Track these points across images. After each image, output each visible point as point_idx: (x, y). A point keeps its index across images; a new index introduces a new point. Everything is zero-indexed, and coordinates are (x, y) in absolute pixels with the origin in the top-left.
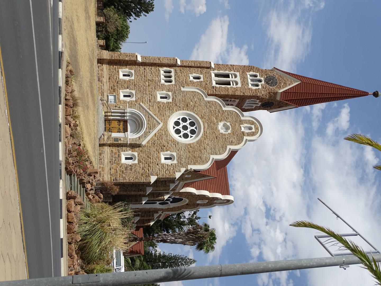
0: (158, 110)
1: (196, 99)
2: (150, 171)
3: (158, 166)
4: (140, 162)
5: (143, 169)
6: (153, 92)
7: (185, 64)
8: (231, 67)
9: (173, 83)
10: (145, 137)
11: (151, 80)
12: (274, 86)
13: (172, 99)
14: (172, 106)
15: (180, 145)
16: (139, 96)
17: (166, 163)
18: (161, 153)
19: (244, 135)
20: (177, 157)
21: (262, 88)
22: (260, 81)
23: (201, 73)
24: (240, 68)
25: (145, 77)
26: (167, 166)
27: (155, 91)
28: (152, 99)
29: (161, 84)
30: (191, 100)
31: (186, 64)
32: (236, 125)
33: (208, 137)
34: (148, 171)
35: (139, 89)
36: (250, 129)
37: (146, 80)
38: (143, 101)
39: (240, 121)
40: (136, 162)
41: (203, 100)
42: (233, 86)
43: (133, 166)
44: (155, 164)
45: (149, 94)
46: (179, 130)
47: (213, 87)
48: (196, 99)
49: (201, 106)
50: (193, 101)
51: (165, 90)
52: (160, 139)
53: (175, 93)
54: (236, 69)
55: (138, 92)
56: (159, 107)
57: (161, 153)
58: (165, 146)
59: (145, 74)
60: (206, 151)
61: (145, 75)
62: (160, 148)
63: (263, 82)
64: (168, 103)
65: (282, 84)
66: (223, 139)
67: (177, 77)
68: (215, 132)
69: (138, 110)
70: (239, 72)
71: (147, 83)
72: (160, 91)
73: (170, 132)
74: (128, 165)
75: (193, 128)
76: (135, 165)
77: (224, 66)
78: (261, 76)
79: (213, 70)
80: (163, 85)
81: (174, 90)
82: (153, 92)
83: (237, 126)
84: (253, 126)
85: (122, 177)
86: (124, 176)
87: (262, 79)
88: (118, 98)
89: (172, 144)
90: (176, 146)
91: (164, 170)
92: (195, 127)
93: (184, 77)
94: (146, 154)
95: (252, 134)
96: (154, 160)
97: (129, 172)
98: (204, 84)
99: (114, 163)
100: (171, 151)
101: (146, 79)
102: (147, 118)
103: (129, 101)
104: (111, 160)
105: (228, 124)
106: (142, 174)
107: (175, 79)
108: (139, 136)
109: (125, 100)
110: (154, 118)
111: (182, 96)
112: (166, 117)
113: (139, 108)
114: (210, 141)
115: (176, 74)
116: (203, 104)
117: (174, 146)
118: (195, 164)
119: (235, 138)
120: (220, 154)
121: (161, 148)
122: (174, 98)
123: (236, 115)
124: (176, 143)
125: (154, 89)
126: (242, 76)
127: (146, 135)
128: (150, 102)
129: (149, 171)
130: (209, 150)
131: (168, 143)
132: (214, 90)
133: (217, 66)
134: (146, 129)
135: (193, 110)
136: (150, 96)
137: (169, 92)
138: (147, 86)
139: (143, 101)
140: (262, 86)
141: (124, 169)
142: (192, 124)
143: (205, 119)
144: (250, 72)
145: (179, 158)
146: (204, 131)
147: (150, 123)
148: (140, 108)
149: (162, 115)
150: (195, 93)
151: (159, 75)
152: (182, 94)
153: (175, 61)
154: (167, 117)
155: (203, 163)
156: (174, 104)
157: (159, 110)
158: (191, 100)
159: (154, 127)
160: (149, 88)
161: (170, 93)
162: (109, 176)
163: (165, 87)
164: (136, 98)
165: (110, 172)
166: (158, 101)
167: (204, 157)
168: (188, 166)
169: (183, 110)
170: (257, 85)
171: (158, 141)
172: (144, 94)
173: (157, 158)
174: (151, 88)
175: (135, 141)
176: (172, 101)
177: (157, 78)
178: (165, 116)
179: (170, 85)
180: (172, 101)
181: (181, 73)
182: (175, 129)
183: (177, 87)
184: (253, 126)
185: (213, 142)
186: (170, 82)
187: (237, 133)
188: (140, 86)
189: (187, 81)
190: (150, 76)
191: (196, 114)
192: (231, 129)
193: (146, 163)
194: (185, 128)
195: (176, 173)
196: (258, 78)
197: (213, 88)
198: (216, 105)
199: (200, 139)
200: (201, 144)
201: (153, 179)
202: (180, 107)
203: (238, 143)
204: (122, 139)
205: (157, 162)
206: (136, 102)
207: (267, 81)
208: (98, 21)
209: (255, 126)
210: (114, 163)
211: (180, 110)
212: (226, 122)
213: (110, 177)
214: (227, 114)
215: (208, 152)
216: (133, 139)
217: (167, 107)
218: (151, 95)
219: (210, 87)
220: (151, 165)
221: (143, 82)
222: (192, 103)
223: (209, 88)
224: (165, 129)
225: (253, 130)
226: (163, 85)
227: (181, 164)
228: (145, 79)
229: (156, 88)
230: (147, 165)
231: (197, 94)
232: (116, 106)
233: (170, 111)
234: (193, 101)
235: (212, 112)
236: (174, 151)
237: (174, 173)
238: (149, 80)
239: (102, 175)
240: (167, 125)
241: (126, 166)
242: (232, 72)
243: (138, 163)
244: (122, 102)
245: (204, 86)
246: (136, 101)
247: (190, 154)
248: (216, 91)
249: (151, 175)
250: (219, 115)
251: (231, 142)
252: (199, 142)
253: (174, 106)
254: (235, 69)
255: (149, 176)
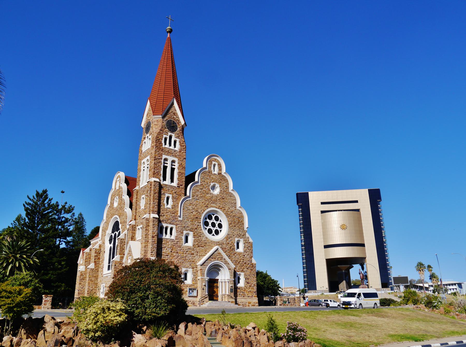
0: (201, 247)
1: (191, 208)
2: (249, 263)
3: (245, 256)
4: (243, 270)
5: (248, 269)
6: (184, 249)
7: (156, 210)
8: (157, 160)
9: (174, 226)
10: (228, 264)
11: (172, 250)
12: (177, 126)
13: (190, 231)
14: (197, 233)
15: (230, 233)
16: (188, 264)
17: (243, 248)
18: (236, 251)
19: (221, 174)
20: (239, 238)
21: (179, 139)
22: (171, 137)
23: (164, 194)
24: (159, 151)
25: (168, 256)
26: (245, 247)
27: (183, 248)
28: (190, 252)
29: (176, 240)
30: (191, 213)
31: (155, 208)
32: (213, 178)
33: (224, 207)
34: (249, 265)
35: (181, 263)
36: (214, 165)
37: (171, 254)
38: (192, 261)
39: (209, 172)
40: (242, 274)
41: (191, 201)
42: (176, 166)
43: (245, 277)
44: (244, 257)
45: (186, 254)
46: (215, 230)
47: (178, 187)
48: (191, 208)
49: (197, 205)
50: (192, 211)
51: (181, 237)
52: (225, 250)
53: (185, 227)
54: (159, 156)
55: (184, 265)
56: (199, 246)
57: (236, 251)
58: (231, 247)
59: (165, 255)
60: (234, 211)
61: (166, 255)
62: (232, 251)
63: (173, 135)
64: (194, 236)
65: (175, 117)
66: (224, 193)
67: (168, 221)
68: (219, 199)
69: (206, 268)
70: (162, 154)
71: (174, 254)
72: (182, 242)
73: (220, 240)
74: (245, 281)
75: (213, 217)
76: (245, 275)
77: (155, 167)
78: (166, 134)
79: (160, 180)
80: (177, 238)
81: (182, 228)
82: (184, 249)
83: (214, 177)
84: (213, 163)
85: (254, 287)
86: (253, 285)
87: (169, 134)
88: (190, 286)
89: (229, 240)
90: (231, 237)
91: (248, 251)
92: (212, 215)
93: (168, 214)
94: (237, 264)
95: (219, 166)
96: (241, 258)
97: (250, 281)
98: (176, 195)
99: (244, 293)
100: (234, 242)
101: (170, 255)
102: (212, 260)
103: (193, 275)
104: (242, 296)
105: (212, 184)
106: (251, 270)
107: (170, 223)
108: (228, 270)
109: (192, 279)
110: (213, 253)
111: (187, 221)
112: (207, 241)
113: (205, 267)
114: (226, 205)
115: (165, 222)
116: (195, 202)
117: (231, 238)
118: (243, 224)
119: (223, 182)
120: (236, 200)
121: (233, 250)
122: (190, 230)
123: (204, 174)
124: (228, 237)
125: (181, 247)
126: (167, 153)
127: (226, 263)
128: (193, 254)
129: (249, 264)
130: (233, 209)
131: (229, 243)
132: (181, 186)
133: (156, 175)
134: (222, 262)
135: (200, 214)
136: (187, 253)
137: (183, 233)
138: (177, 254)
139: (192, 261)
140: (177, 138)
141: (248, 285)
142: (210, 217)
143: (208, 204)
144: (162, 143)
145: (239, 236)
146: (219, 208)
147: (217, 257)
148: (204, 265)
149: (205, 244)
150: (185, 207)
151: (166, 239)
152: (186, 221)
153: (155, 219)
154: (207, 240)
155: (242, 217)
156: (195, 231)
157: (201, 247)
158: (191, 213)
159: (220, 254)
160: (180, 253)
161: (185, 232)
162: (253, 298)
163: (179, 236)
164: (190, 267)
165: (251, 297)
166: (192, 246)
167: (238, 215)
168: (245, 230)
169: (200, 223)
170: (175, 142)
171: (227, 252)
172: (185, 259)
173: (240, 255)
174: (180, 251)
175: (232, 273)
176: (192, 233)
177: (168, 242)
178: (206, 242)
179: (176, 231)
180: (192, 231)
181: (163, 215)
182: (215, 234)
183: (179, 223)
184: (213, 163)
185: (226, 203)
186: (171, 229)
187: (219, 179)
188: (178, 262)
189: (172, 212)
190: (166, 249)
191: (204, 211)
192: (216, 184)
193: (244, 265)
194: (213, 225)
195: (250, 241)
196: (168, 137)
197: (179, 187)
198: (195, 190)
199: (225, 214)
200: (228, 214)
201: (254, 261)
202: (198, 225)
203: (227, 181)
204: (231, 285)
205: (243, 256)
206: (194, 268)
207: (172, 130)
208: (50, 304)
209: (213, 161)
210: (244, 293)
211: (200, 226)
212: (210, 186)
213: (254, 297)
214: (203, 182)
215: (234, 210)
216: (230, 275)
217: (198, 238)
218: (187, 251)
219: (178, 190)
220: (245, 261)
221: (173, 258)
222: (194, 213)
223: (179, 191)
224: (218, 243)
225: (217, 163)
226: (177, 238)
227: (244, 236)
228: (170, 256)
229: (180, 246)
230: (245, 265)
231: (186, 205)
232: (203, 289)
233: (201, 236)
234: (192, 211)
235: (201, 195)
236: (234, 239)
237: (250, 243)
238: (171, 251)
239: (254, 304)
240: (214, 242)
241: (246, 283)
242: (162, 161)
243: (244, 272)
244: (194, 282)
245: (177, 196)
246: (193, 268)
247: (236, 226)
248: (182, 185)
249: (252, 262)
250: (204, 189)
251: (226, 187)
252: (227, 215)
253: (197, 231)
254: (159, 158)
255: (253, 264)
